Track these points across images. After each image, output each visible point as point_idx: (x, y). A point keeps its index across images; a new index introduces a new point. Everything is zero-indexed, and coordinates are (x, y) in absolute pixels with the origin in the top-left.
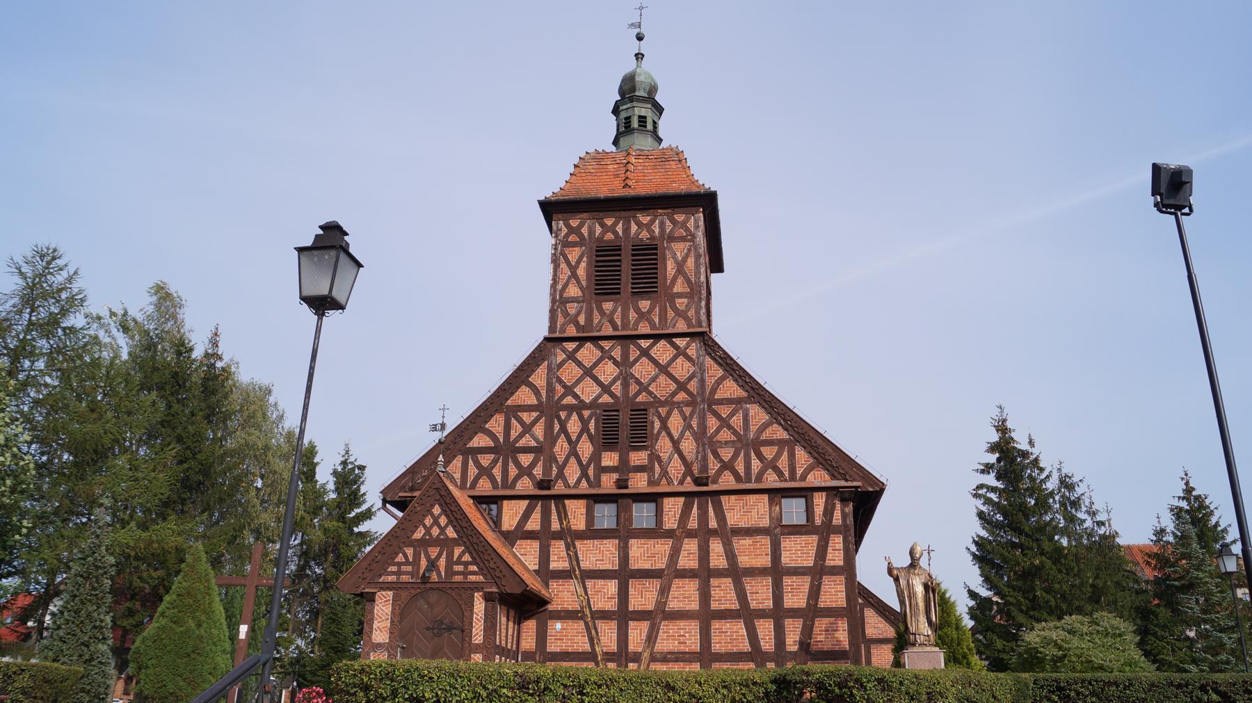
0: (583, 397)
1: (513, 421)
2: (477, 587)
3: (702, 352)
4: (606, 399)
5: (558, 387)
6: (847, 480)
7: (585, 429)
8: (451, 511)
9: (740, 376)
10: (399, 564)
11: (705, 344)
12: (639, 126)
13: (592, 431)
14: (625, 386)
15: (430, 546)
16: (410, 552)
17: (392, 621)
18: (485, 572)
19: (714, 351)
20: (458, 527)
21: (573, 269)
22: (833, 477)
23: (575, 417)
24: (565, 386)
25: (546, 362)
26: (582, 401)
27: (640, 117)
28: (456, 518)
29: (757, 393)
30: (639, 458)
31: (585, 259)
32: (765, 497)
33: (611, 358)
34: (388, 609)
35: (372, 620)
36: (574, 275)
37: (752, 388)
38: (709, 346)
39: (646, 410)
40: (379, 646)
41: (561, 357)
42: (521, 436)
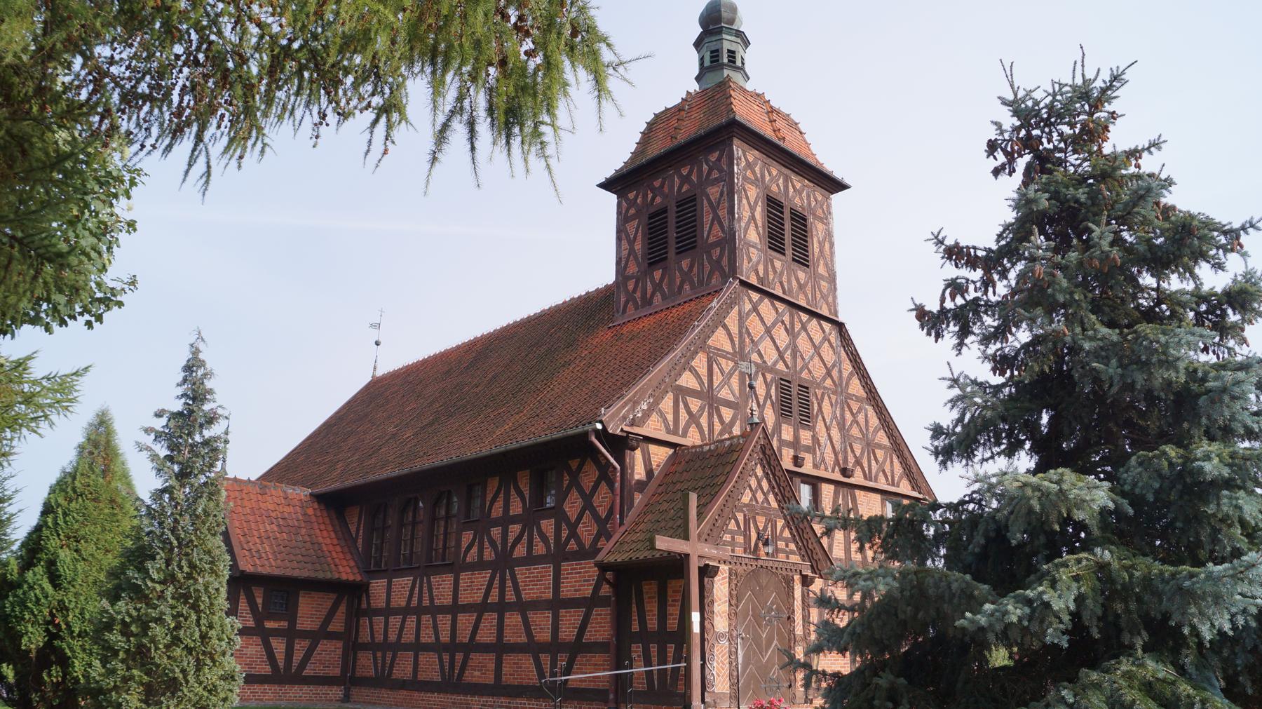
0: (766, 359)
1: (715, 366)
2: (795, 568)
3: (839, 343)
4: (781, 366)
5: (747, 340)
6: (920, 493)
7: (768, 395)
8: (774, 475)
9: (863, 376)
10: (732, 533)
11: (841, 335)
12: (729, 61)
13: (773, 397)
14: (794, 356)
15: (758, 514)
16: (740, 517)
17: (730, 605)
18: (803, 552)
19: (848, 345)
20: (779, 497)
21: (752, 209)
22: (913, 489)
23: (760, 378)
24: (752, 341)
25: (736, 308)
26: (765, 362)
27: (729, 51)
28: (779, 485)
29: (872, 396)
30: (806, 437)
31: (760, 203)
32: (878, 497)
33: (783, 322)
34: (726, 590)
35: (712, 602)
36: (753, 217)
37: (870, 391)
38: (845, 338)
39: (807, 388)
40: (722, 635)
41: (748, 306)
42: (721, 386)
